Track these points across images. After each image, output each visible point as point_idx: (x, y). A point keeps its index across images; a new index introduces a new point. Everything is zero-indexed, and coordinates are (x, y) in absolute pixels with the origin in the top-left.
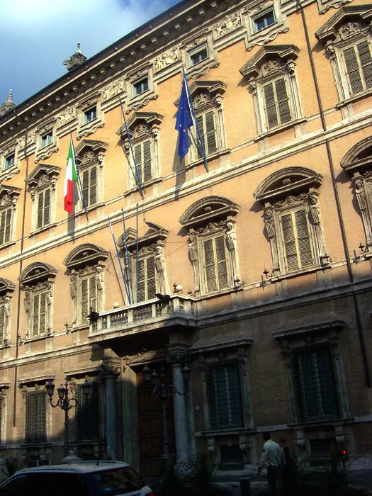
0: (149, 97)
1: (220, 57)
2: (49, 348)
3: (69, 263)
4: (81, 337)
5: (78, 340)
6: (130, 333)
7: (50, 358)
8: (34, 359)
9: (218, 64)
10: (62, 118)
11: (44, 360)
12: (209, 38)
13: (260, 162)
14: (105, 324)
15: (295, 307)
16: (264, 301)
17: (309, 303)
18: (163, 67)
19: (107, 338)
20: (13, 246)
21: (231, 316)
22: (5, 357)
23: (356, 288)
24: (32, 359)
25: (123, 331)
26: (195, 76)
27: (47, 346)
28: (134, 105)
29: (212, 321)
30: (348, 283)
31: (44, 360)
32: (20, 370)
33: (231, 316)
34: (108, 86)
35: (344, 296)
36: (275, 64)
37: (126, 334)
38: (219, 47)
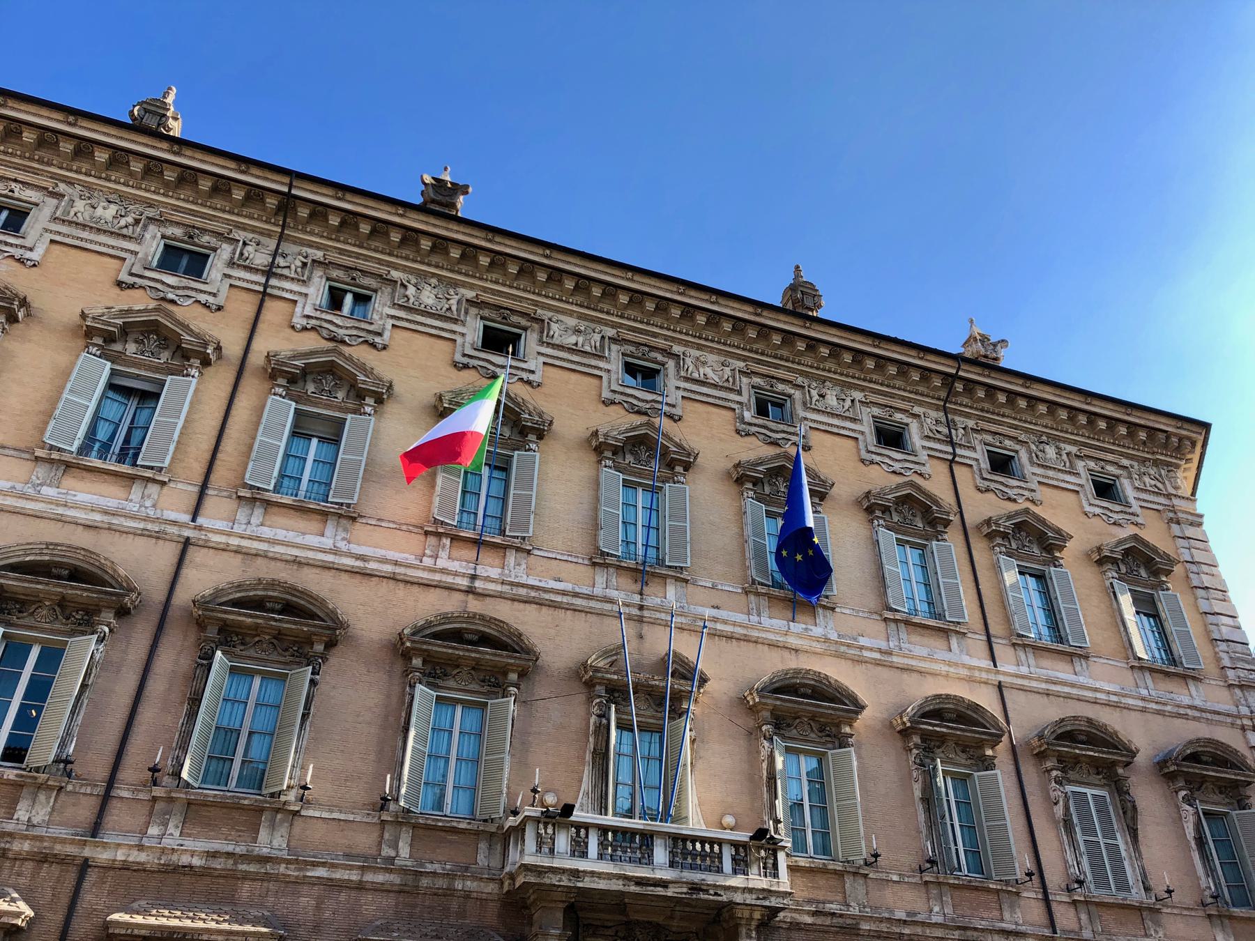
1: (816, 438)
2: (271, 841)
3: (416, 638)
4: (411, 845)
5: (404, 850)
6: (660, 891)
7: (267, 877)
11: (246, 876)
12: (797, 394)
14: (579, 849)
16: (908, 914)
18: (696, 375)
19: (587, 883)
20: (153, 489)
21: (849, 921)
22: (22, 813)
25: (640, 882)
26: (761, 437)
27: (263, 835)
28: (625, 398)
29: (808, 919)
32: (102, 881)
37: (650, 890)
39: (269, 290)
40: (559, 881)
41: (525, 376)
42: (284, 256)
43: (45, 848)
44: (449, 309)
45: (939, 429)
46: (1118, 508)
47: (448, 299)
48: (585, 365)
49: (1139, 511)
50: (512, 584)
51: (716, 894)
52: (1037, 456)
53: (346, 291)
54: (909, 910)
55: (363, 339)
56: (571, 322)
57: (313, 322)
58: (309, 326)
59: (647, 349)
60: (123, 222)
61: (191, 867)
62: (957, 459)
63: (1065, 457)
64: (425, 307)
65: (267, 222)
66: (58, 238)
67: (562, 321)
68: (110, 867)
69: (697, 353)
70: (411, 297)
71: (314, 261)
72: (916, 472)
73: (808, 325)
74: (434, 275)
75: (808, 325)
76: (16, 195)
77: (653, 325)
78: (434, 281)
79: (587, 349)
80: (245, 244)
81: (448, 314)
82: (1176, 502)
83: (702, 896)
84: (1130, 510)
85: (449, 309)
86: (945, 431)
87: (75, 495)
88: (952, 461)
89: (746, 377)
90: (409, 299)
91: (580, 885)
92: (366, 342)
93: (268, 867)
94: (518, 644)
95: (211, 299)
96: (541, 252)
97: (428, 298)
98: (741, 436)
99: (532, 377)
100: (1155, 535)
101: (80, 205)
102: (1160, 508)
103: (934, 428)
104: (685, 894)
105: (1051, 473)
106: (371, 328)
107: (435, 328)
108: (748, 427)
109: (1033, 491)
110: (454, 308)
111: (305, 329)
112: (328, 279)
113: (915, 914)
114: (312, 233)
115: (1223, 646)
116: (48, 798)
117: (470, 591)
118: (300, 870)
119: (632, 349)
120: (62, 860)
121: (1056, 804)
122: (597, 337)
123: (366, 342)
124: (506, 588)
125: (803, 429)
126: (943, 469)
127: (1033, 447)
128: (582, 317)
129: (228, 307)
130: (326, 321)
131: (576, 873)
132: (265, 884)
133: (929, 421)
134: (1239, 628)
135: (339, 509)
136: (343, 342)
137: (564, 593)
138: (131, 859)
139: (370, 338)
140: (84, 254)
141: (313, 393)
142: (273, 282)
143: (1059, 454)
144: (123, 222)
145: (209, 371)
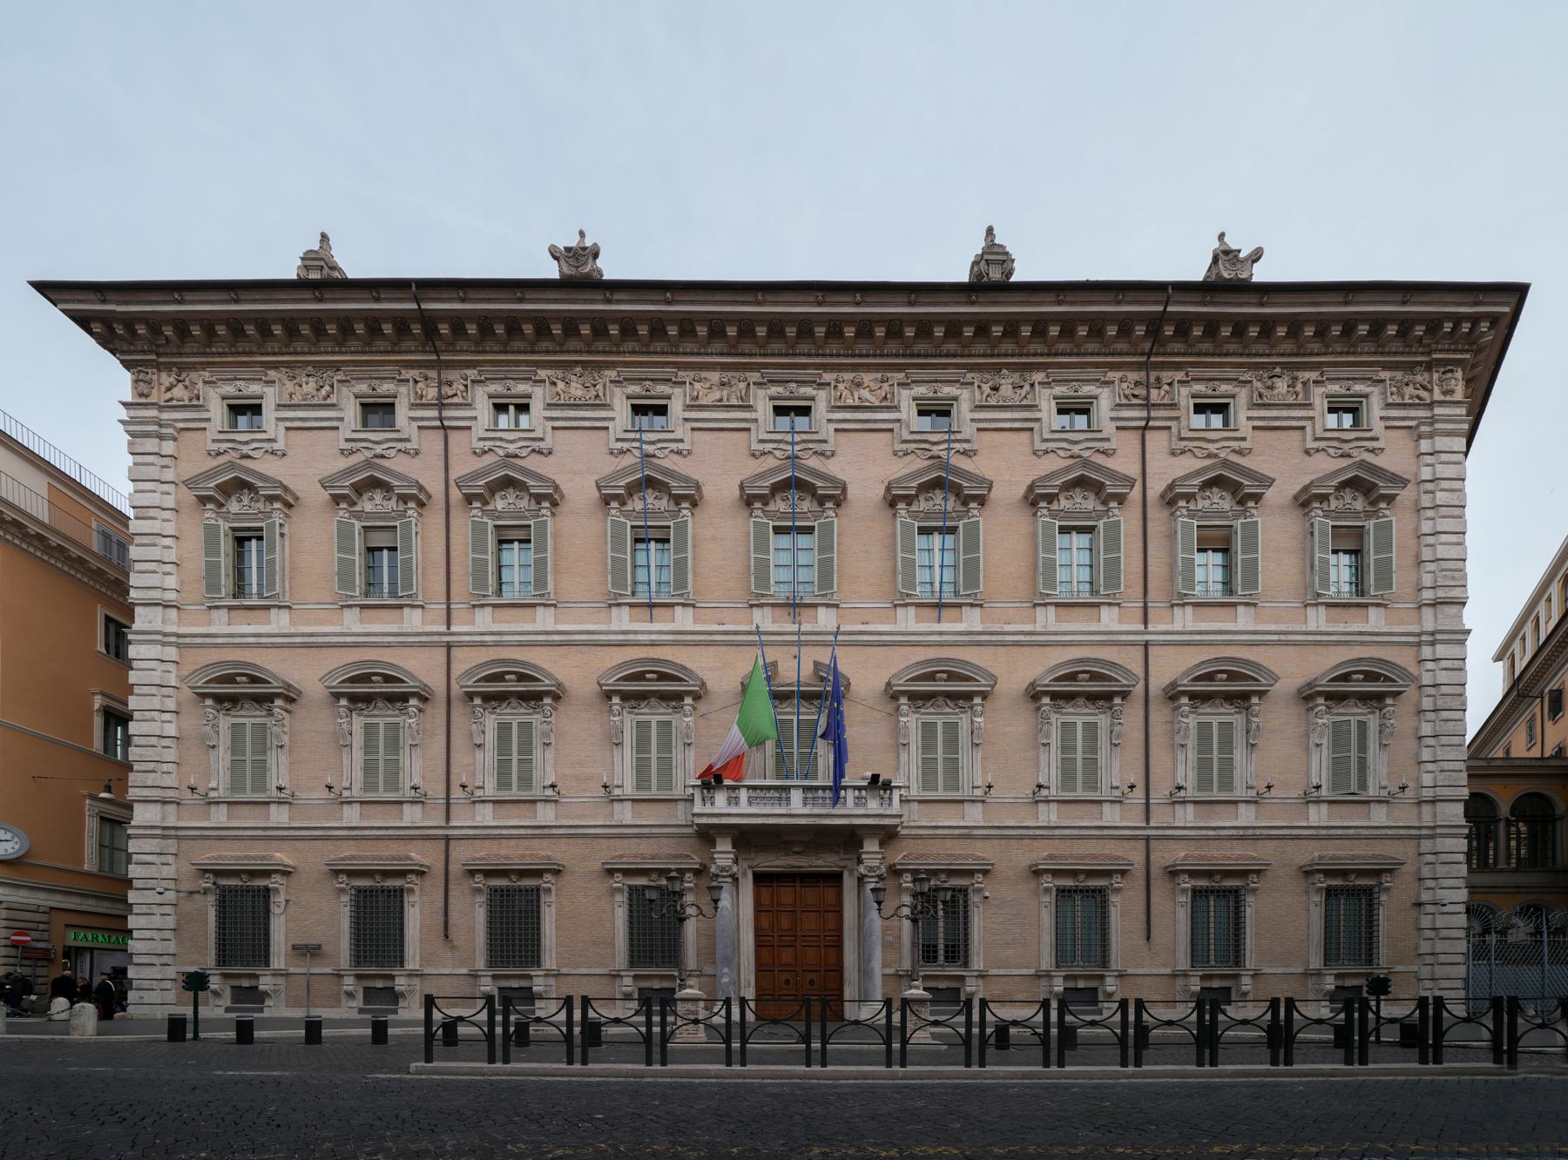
0: (810, 446)
9: (975, 452)
10: (561, 385)
18: (850, 402)
28: (775, 446)
34: (704, 374)
36: (1084, 498)
38: (980, 420)
39: (446, 423)
41: (674, 446)
42: (450, 384)
44: (597, 396)
45: (1136, 393)
47: (595, 386)
52: (1260, 395)
55: (530, 449)
56: (715, 376)
57: (488, 444)
59: (794, 385)
60: (323, 392)
63: (1299, 387)
65: (425, 352)
66: (289, 424)
67: (705, 379)
69: (849, 376)
70: (561, 393)
71: (473, 381)
72: (1098, 451)
74: (577, 363)
76: (245, 392)
77: (800, 355)
78: (578, 369)
79: (734, 402)
80: (416, 382)
81: (597, 402)
85: (597, 396)
86: (1144, 392)
88: (1145, 428)
92: (534, 450)
96: (662, 298)
97: (576, 390)
98: (900, 457)
99: (681, 446)
100: (1394, 455)
101: (290, 386)
102: (1413, 423)
103: (1128, 392)
108: (905, 446)
110: (601, 394)
112: (490, 397)
114: (461, 352)
119: (780, 389)
122: (742, 385)
123: (534, 450)
126: (1133, 439)
127: (1259, 384)
128: (725, 367)
129: (424, 449)
133: (1124, 385)
136: (516, 456)
140: (311, 433)
142: (446, 413)
144: (323, 392)
145: (425, 512)
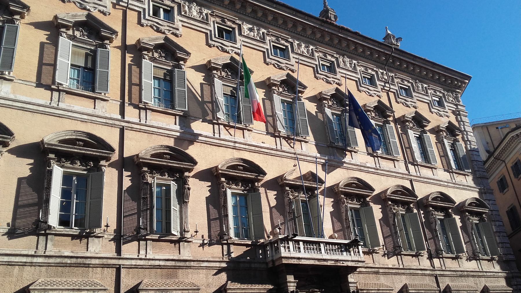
6: (325, 263)
8: (162, 263)
11: (180, 267)
13: (379, 171)
15: (411, 274)
17: (417, 274)
23: (438, 273)
24: (157, 263)
25: (319, 260)
26: (325, 80)
30: (432, 268)
31: (180, 267)
33: (376, 270)
35: (432, 275)
40: (294, 262)
43: (104, 262)
46: (442, 110)
48: (257, 46)
49: (449, 111)
50: (249, 145)
51: (343, 263)
53: (160, 7)
54: (392, 264)
58: (149, 25)
61: (160, 266)
62: (391, 90)
64: (194, 17)
68: (130, 267)
73: (340, 31)
75: (340, 31)
82: (459, 107)
83: (339, 264)
84: (446, 111)
87: (73, 107)
89: (317, 53)
90: (186, 13)
91: (300, 263)
93: (188, 264)
94: (258, 170)
95: (105, 9)
104: (333, 264)
105: (420, 96)
106: (174, 26)
107: (199, 27)
109: (415, 103)
111: (147, 26)
113: (395, 265)
115: (475, 163)
116: (99, 241)
117: (234, 148)
118: (198, 264)
120: (108, 266)
121: (432, 223)
124: (247, 147)
125: (338, 76)
130: (155, 22)
131: (299, 258)
132: (187, 270)
134: (479, 156)
135: (180, 113)
137: (268, 149)
138: (138, 264)
139: (175, 31)
141: (158, 58)
143: (422, 87)
